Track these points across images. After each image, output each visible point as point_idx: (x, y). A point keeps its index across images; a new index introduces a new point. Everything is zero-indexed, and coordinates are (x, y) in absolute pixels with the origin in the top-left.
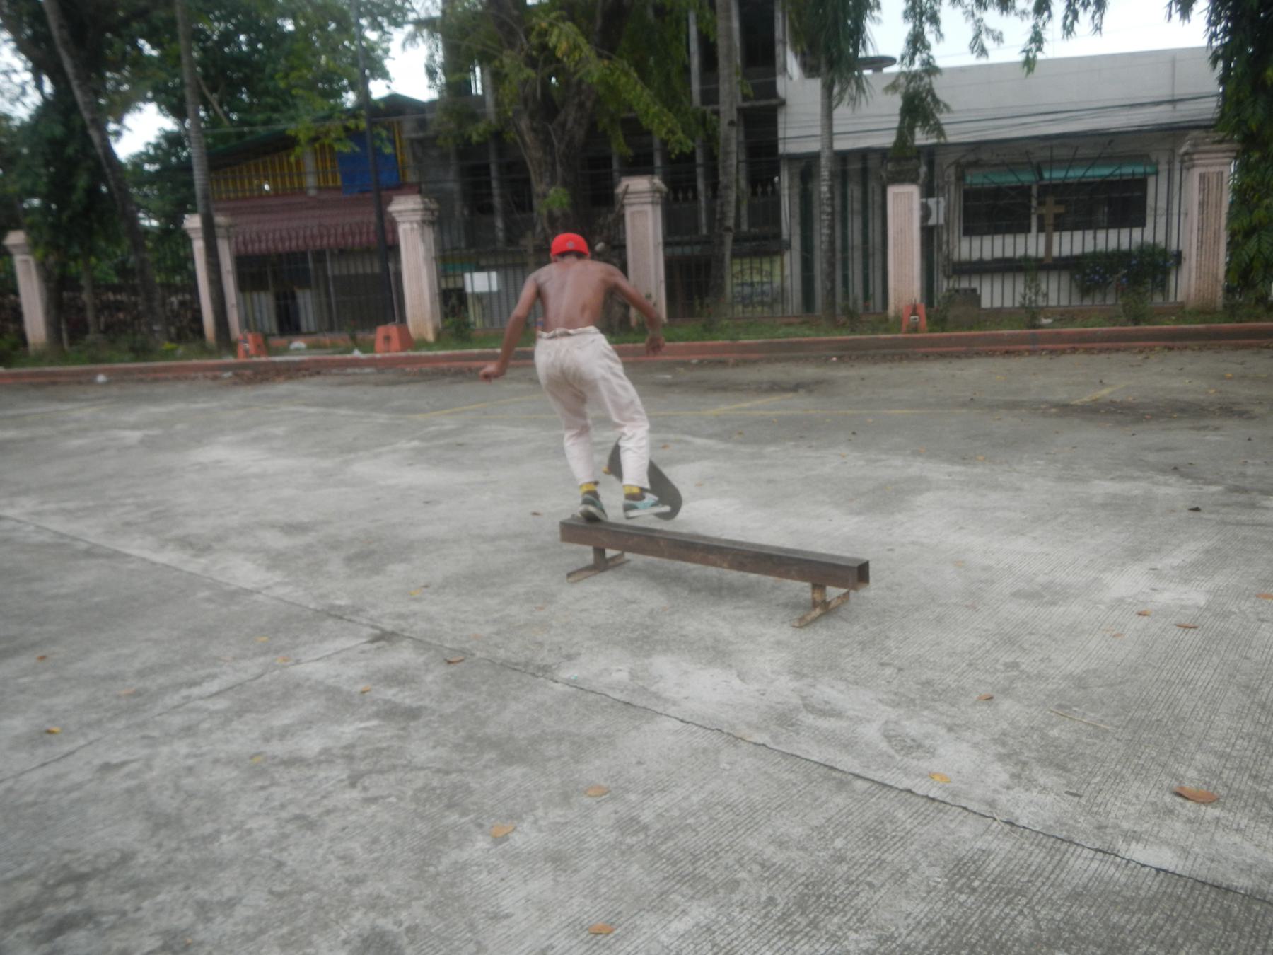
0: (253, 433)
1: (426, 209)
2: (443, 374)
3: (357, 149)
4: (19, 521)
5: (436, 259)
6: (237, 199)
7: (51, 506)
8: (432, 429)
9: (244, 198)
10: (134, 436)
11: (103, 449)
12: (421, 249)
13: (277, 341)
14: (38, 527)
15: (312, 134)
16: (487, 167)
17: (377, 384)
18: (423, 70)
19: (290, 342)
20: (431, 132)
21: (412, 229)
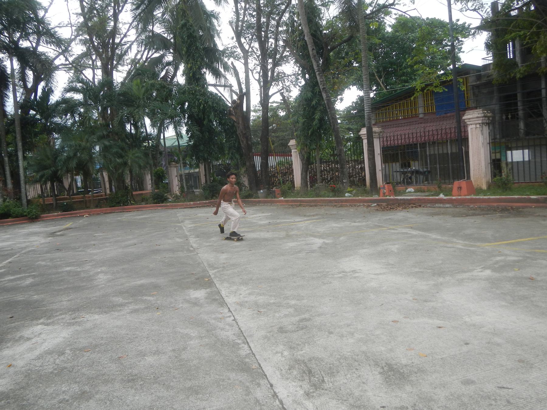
0: (379, 248)
1: (485, 117)
2: (495, 210)
3: (446, 90)
4: (230, 311)
5: (489, 143)
6: (386, 121)
7: (252, 298)
8: (498, 258)
9: (390, 121)
10: (318, 242)
11: (300, 252)
12: (481, 139)
13: (400, 188)
14: (235, 320)
15: (423, 85)
16: (516, 95)
17: (454, 216)
18: (484, 45)
19: (407, 189)
20: (484, 80)
21: (476, 128)
